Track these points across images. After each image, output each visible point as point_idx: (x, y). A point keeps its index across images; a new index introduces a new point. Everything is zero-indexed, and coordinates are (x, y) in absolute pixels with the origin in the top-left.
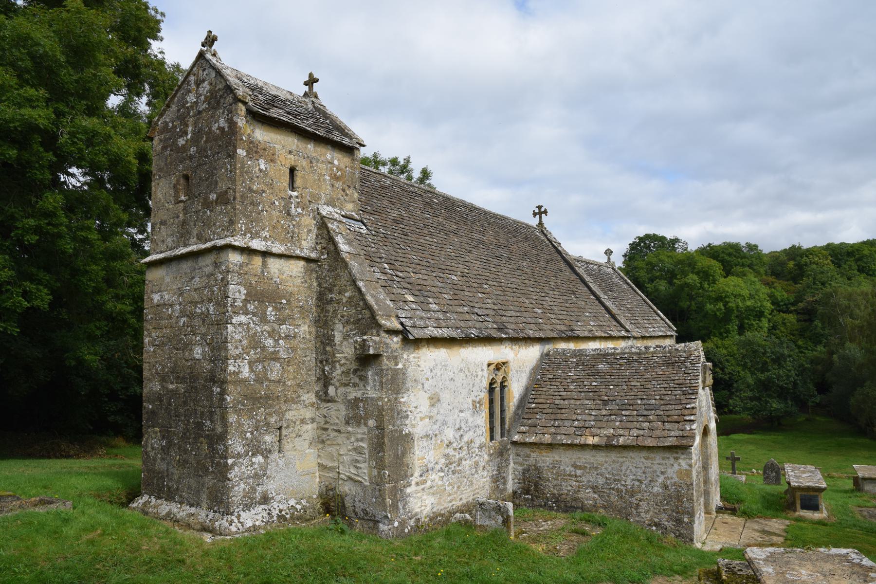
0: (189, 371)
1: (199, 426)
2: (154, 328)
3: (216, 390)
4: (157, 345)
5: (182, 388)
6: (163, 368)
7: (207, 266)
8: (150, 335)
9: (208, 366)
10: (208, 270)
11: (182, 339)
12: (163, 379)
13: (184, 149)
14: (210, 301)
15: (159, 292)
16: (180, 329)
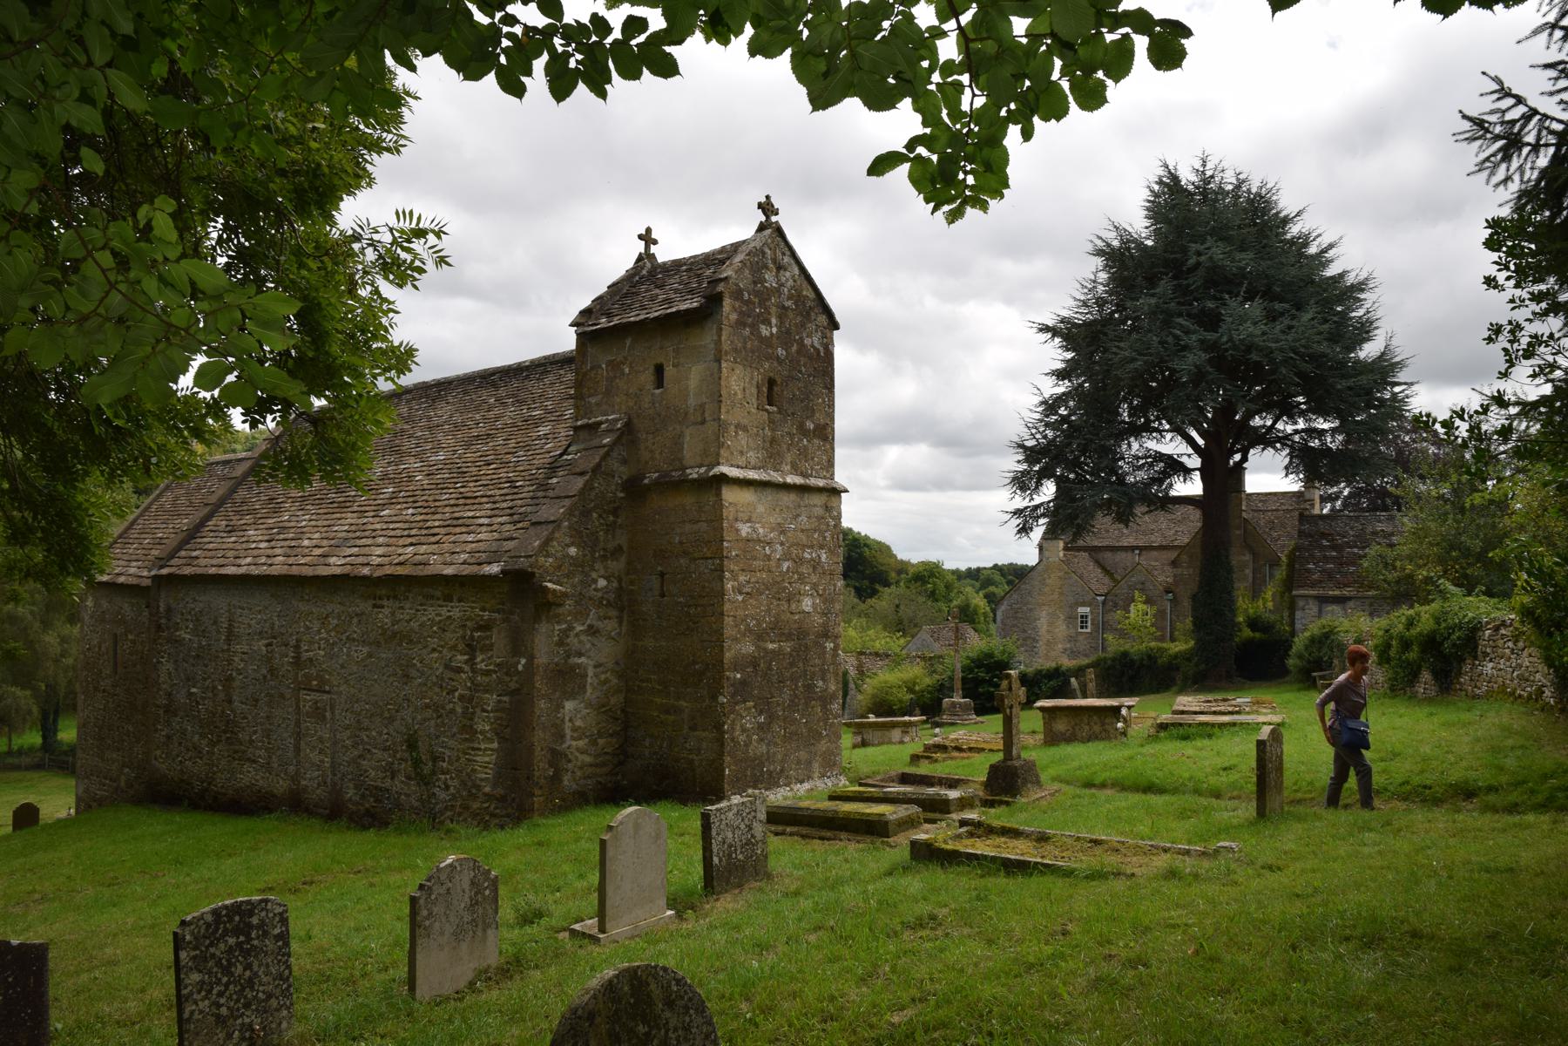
0: (796, 626)
1: (809, 688)
3: (829, 645)
4: (748, 593)
5: (787, 647)
6: (759, 624)
7: (815, 506)
8: (735, 578)
9: (818, 620)
10: (819, 511)
11: (786, 588)
12: (760, 637)
14: (821, 547)
15: (749, 521)
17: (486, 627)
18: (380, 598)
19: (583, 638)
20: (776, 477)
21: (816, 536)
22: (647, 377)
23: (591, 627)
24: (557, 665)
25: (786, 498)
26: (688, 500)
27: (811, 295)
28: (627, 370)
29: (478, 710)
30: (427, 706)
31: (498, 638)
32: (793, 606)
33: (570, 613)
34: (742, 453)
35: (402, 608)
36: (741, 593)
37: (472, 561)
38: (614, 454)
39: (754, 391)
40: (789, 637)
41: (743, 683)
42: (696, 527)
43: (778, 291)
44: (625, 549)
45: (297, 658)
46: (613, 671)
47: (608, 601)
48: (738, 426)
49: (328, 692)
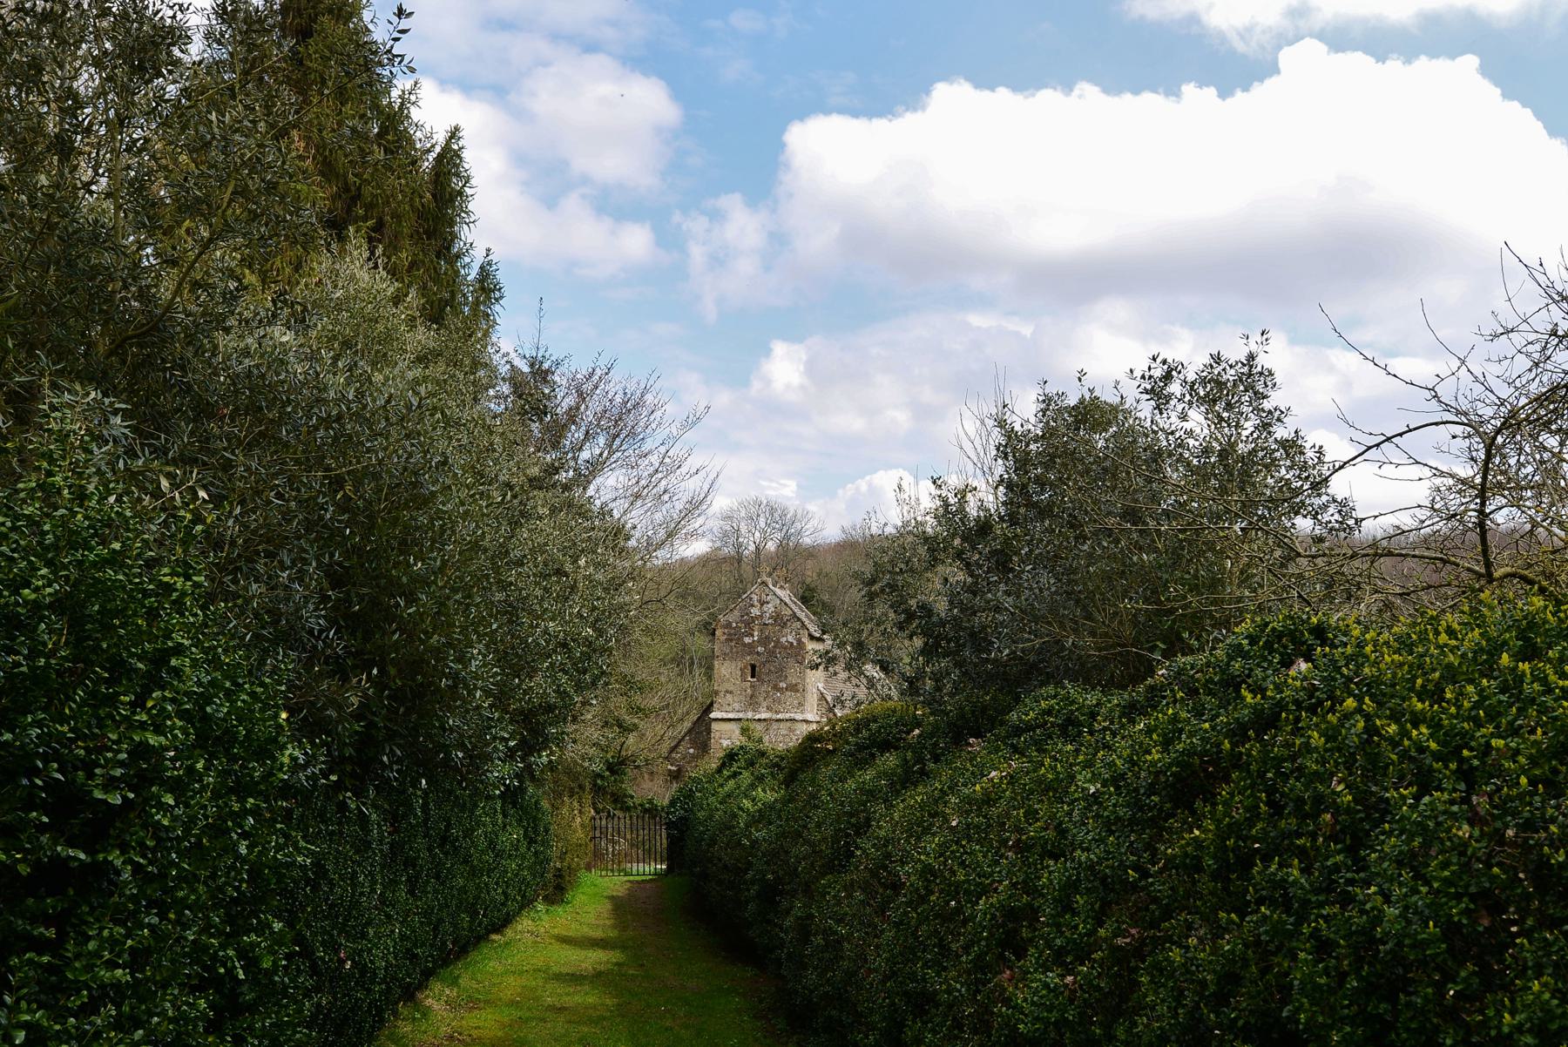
43: (761, 616)
48: (727, 692)
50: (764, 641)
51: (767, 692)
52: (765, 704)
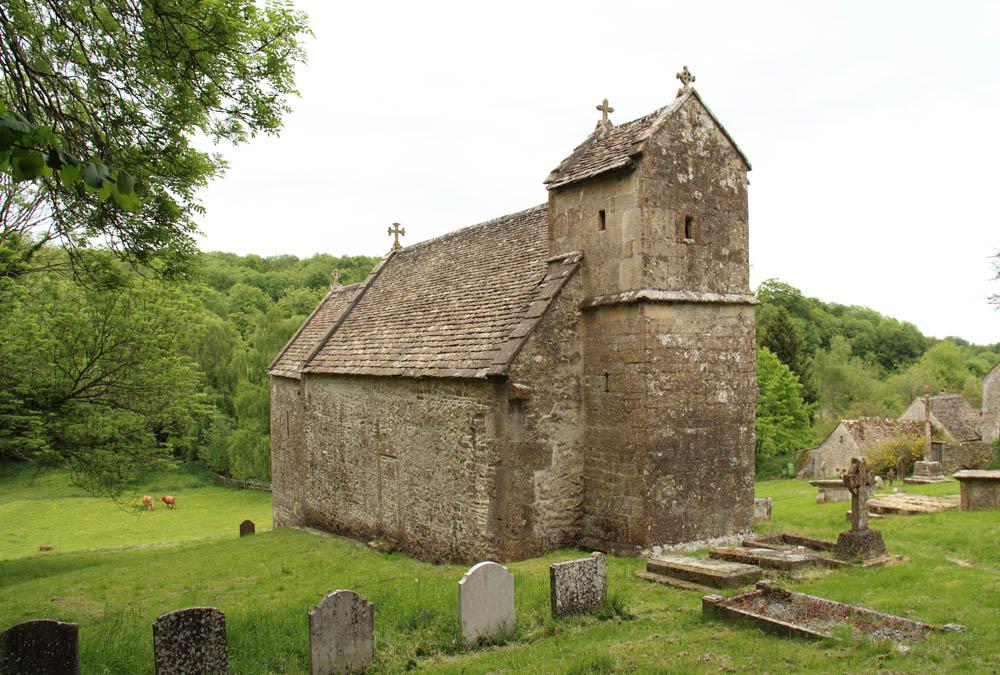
1: (725, 463)
2: (664, 372)
4: (668, 390)
5: (703, 431)
6: (678, 413)
7: (731, 317)
10: (733, 321)
13: (686, 187)
14: (736, 350)
15: (668, 333)
16: (700, 374)
17: (480, 415)
18: (421, 392)
19: (547, 424)
20: (694, 296)
21: (731, 341)
22: (595, 220)
23: (554, 415)
24: (527, 444)
25: (702, 313)
26: (622, 317)
27: (726, 144)
28: (581, 217)
29: (478, 476)
30: (449, 471)
31: (488, 423)
32: (710, 399)
33: (537, 404)
34: (663, 279)
35: (433, 399)
36: (662, 390)
37: (472, 366)
38: (572, 283)
39: (673, 228)
40: (706, 424)
41: (665, 460)
42: (628, 339)
43: (693, 145)
44: (582, 354)
45: (378, 432)
46: (573, 448)
47: (568, 395)
49: (395, 458)
50: (701, 182)
51: (708, 261)
52: (705, 280)
